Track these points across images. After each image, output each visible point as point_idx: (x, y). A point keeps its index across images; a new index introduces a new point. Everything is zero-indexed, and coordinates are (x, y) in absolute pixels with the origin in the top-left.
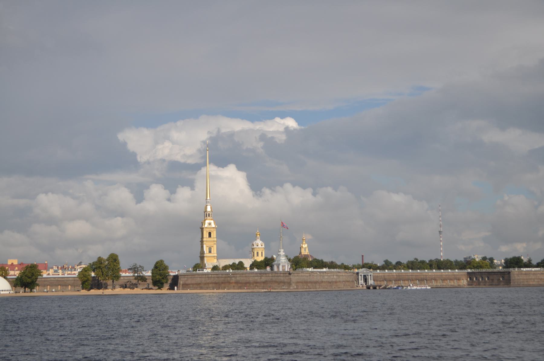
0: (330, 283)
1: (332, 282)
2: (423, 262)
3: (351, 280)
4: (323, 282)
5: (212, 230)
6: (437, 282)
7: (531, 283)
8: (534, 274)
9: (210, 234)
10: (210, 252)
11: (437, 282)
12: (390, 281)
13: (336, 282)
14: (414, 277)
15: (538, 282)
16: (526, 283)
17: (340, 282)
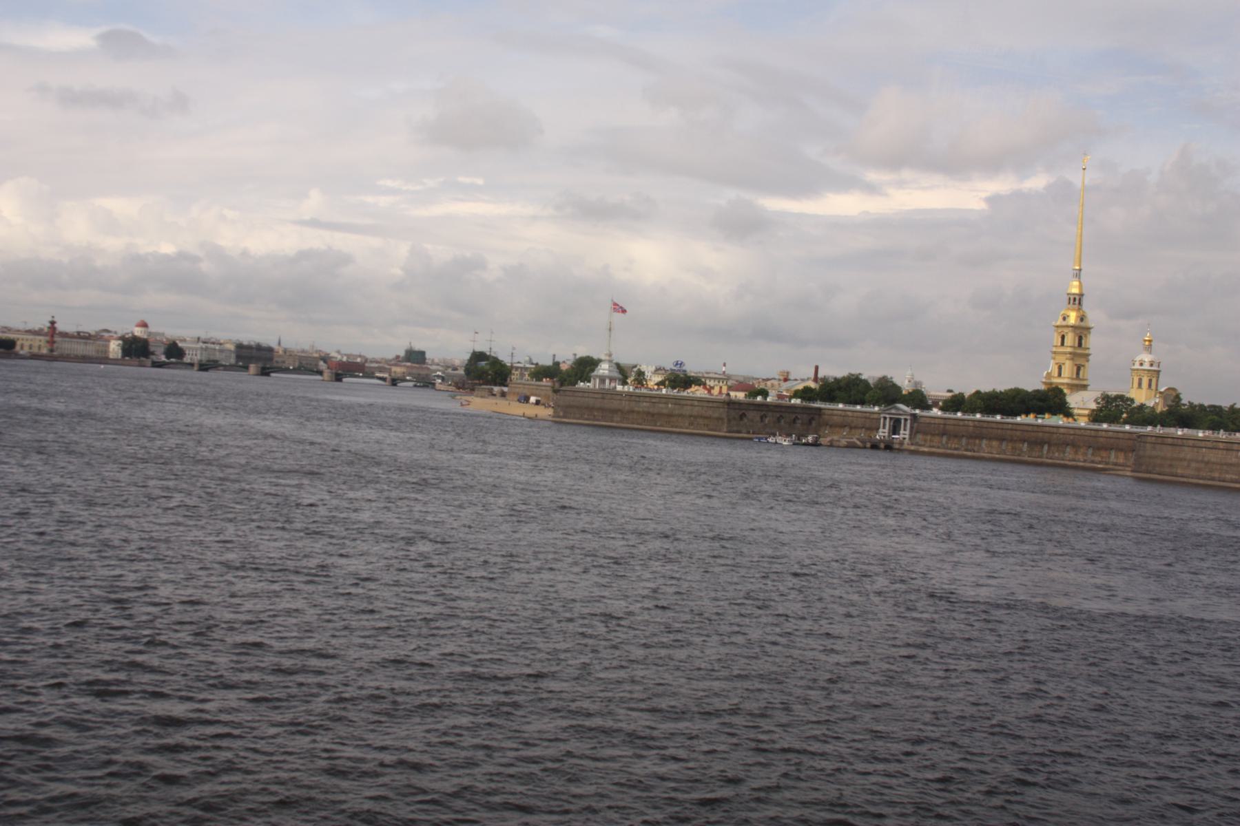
0: (653, 415)
1: (660, 415)
2: (1217, 410)
3: (716, 415)
4: (633, 412)
5: (1066, 330)
6: (1076, 452)
7: (1179, 471)
8: (1194, 446)
9: (1063, 337)
10: (1060, 375)
11: (1076, 452)
12: (956, 436)
13: (670, 415)
14: (1018, 433)
15: (1198, 470)
16: (1167, 470)
17: (680, 415)
